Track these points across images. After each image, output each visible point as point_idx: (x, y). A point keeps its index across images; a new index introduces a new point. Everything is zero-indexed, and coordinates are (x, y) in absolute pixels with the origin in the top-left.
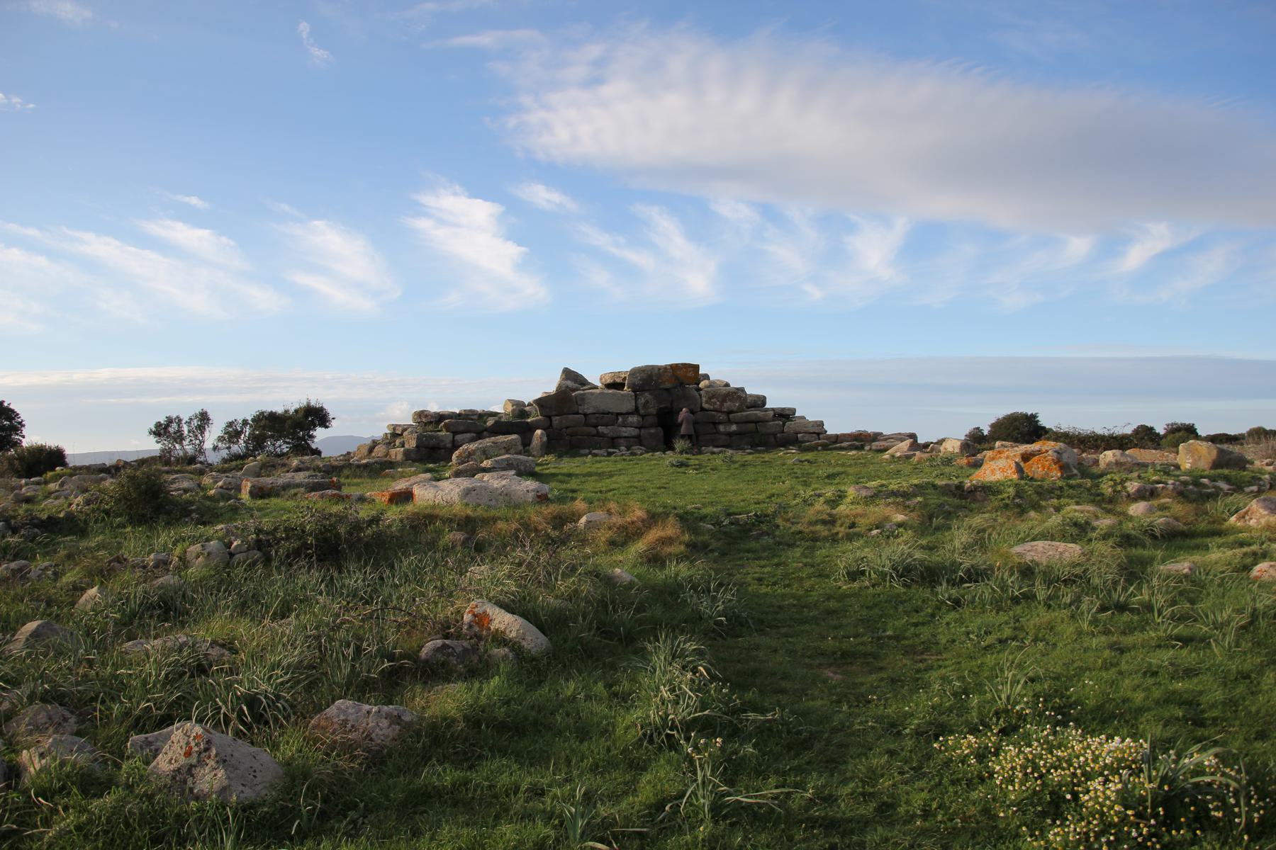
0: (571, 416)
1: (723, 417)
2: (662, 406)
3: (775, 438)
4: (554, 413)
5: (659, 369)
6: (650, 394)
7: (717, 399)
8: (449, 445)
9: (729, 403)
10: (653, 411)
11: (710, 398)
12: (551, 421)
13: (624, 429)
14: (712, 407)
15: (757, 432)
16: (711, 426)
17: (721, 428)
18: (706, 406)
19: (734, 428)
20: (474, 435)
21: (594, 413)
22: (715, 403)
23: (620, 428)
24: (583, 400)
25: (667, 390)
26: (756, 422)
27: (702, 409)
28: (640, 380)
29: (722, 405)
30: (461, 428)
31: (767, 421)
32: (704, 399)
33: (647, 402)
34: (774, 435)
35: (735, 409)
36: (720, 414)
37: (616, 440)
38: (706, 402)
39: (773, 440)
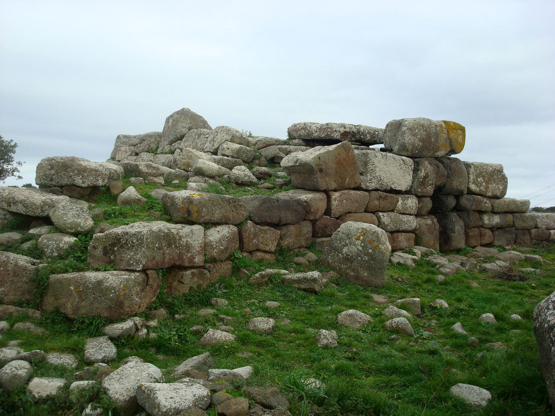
0: (352, 192)
1: (487, 204)
2: (438, 184)
3: (530, 233)
4: (334, 185)
5: (436, 126)
6: (430, 164)
7: (484, 177)
8: (198, 260)
9: (494, 185)
10: (430, 190)
11: (477, 176)
12: (329, 198)
13: (405, 218)
14: (478, 190)
15: (513, 226)
16: (478, 215)
17: (486, 219)
18: (473, 187)
19: (496, 220)
20: (235, 229)
21: (376, 190)
22: (481, 184)
23: (401, 216)
24: (366, 164)
25: (437, 158)
26: (512, 213)
27: (470, 192)
28: (420, 140)
29: (487, 188)
30: (217, 215)
31: (522, 213)
32: (472, 177)
33: (426, 177)
34: (529, 230)
35: (498, 193)
36: (485, 200)
37: (395, 235)
38: (474, 183)
39: (527, 237)
